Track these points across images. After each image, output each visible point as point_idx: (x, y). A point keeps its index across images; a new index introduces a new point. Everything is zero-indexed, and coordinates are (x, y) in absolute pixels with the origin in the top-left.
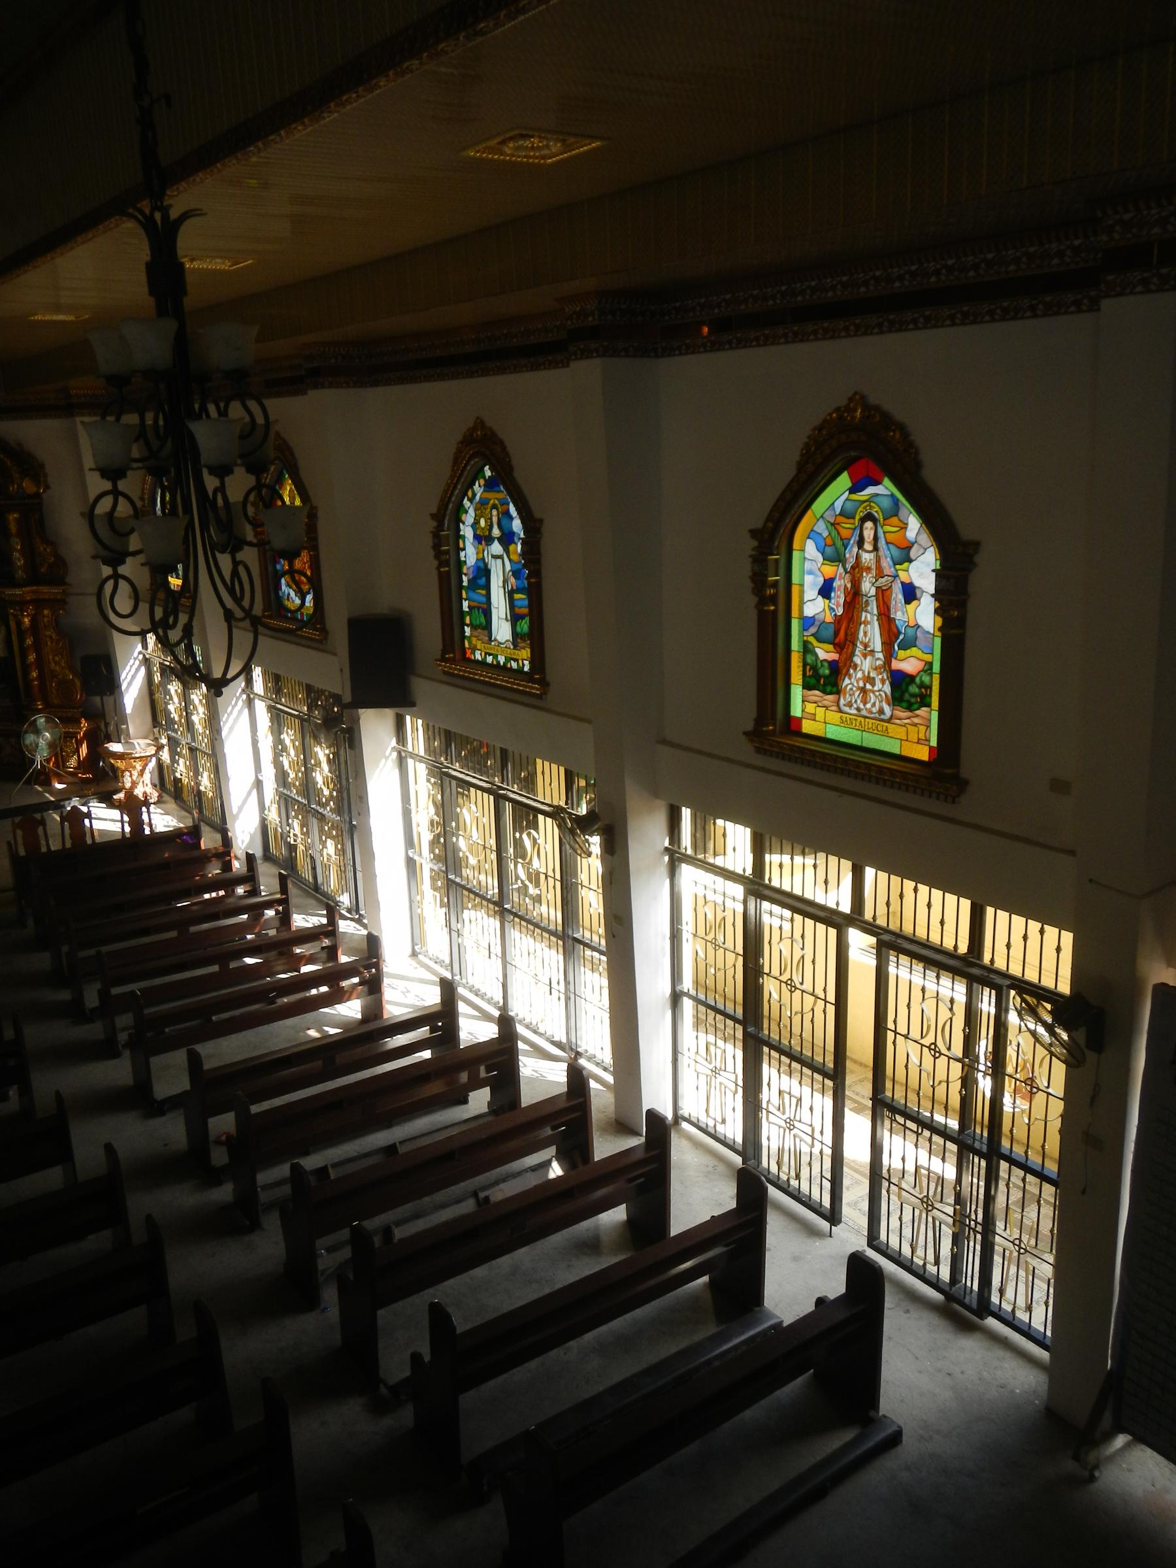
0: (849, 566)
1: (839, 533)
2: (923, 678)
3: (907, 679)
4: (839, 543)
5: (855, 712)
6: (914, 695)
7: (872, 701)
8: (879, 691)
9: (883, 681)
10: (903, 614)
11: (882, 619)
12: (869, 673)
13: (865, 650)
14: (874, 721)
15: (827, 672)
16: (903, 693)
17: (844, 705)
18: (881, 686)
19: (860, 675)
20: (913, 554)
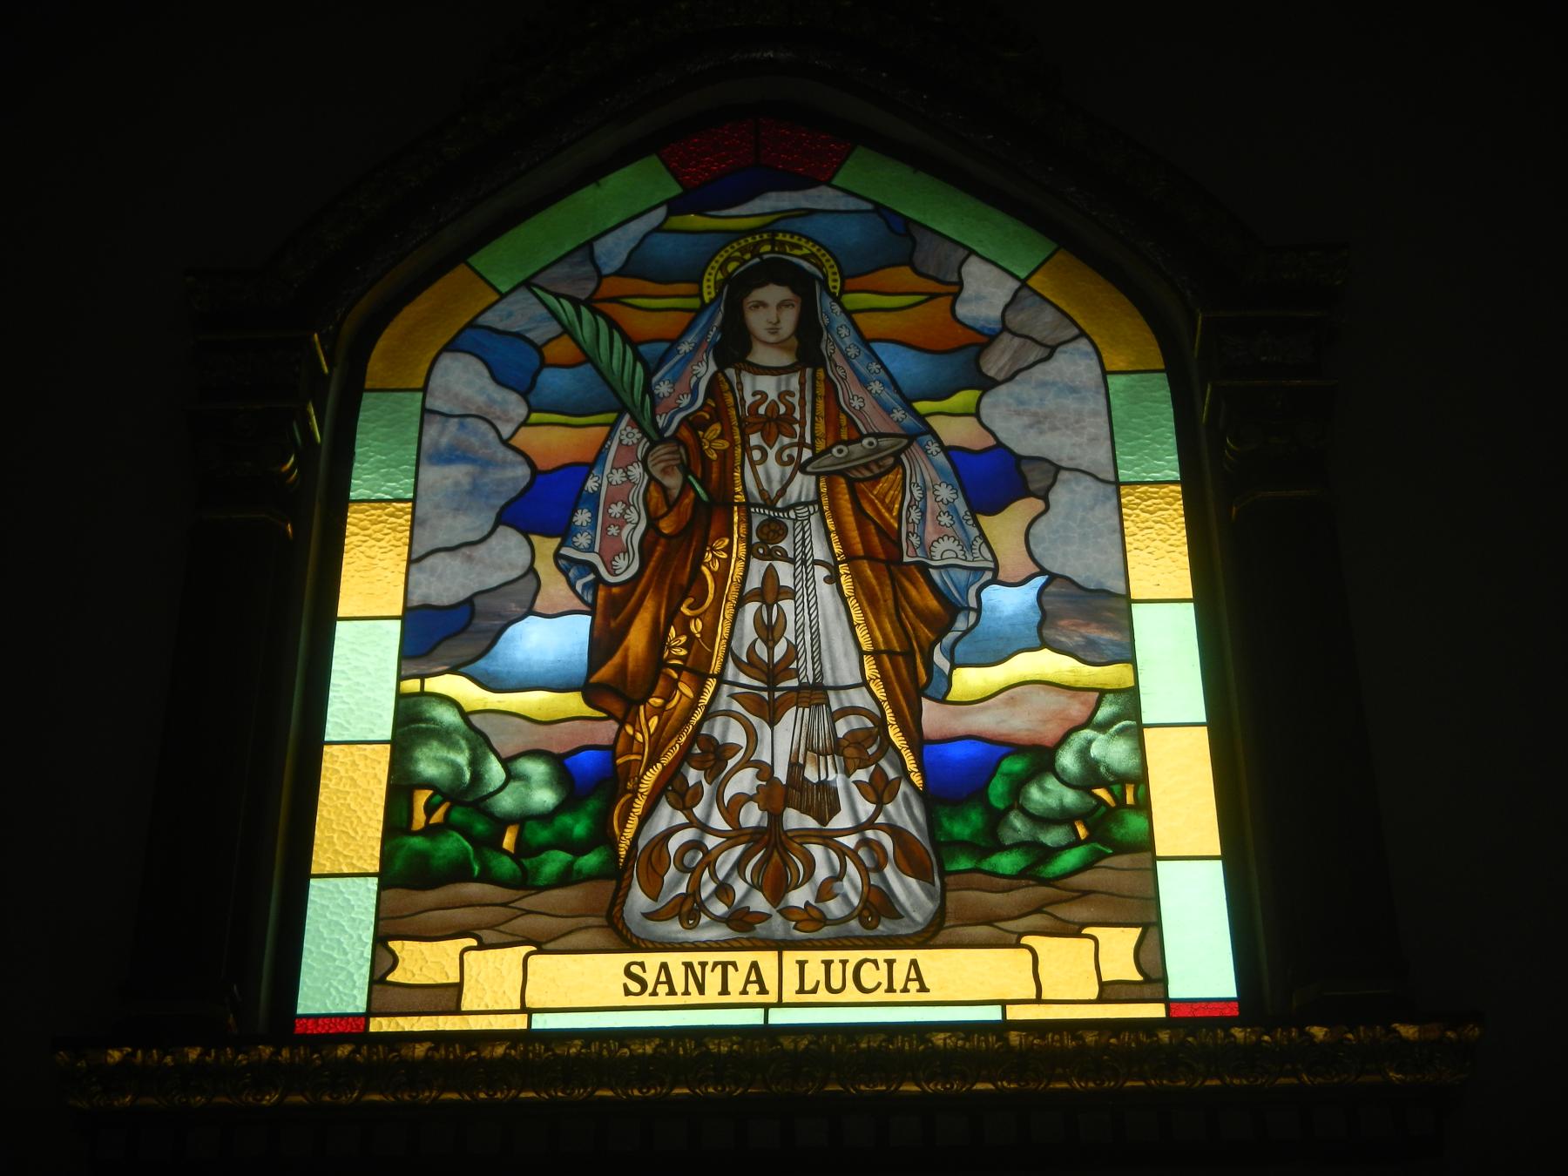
0: (669, 422)
1: (613, 324)
2: (1095, 751)
3: (1013, 765)
4: (616, 357)
5: (719, 933)
6: (1064, 818)
7: (822, 873)
8: (871, 824)
9: (880, 791)
10: (968, 546)
11: (857, 576)
12: (795, 767)
13: (771, 688)
14: (854, 956)
15: (544, 798)
16: (996, 819)
17: (648, 916)
18: (866, 809)
19: (743, 782)
20: (994, 364)
